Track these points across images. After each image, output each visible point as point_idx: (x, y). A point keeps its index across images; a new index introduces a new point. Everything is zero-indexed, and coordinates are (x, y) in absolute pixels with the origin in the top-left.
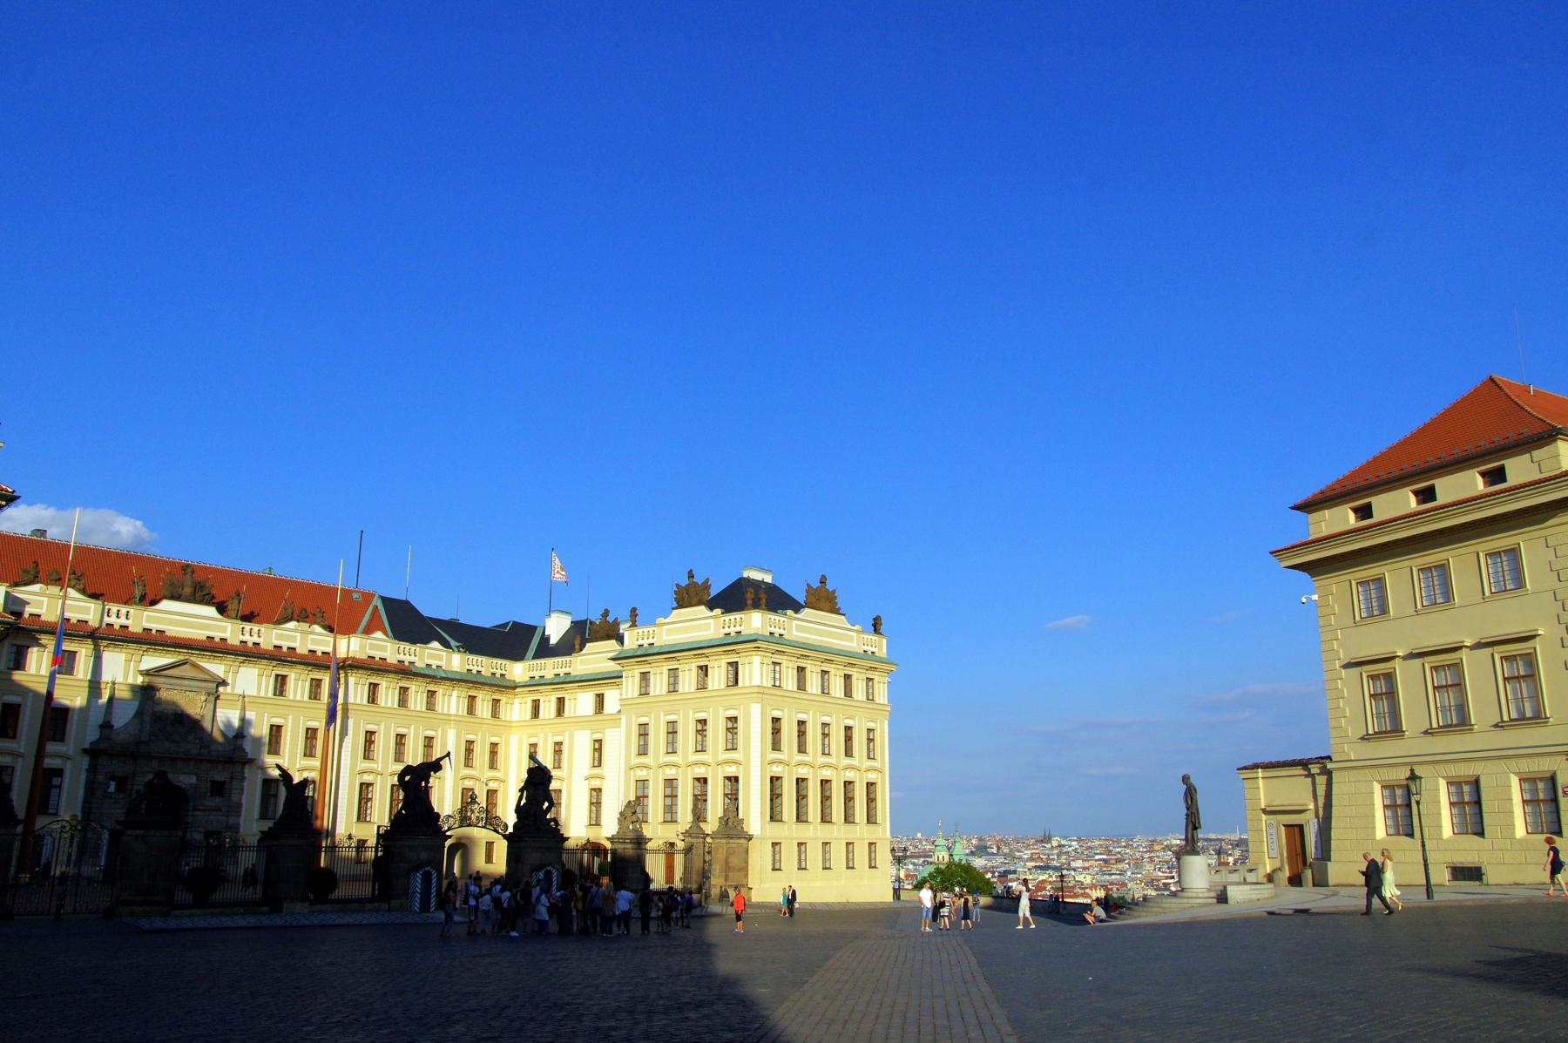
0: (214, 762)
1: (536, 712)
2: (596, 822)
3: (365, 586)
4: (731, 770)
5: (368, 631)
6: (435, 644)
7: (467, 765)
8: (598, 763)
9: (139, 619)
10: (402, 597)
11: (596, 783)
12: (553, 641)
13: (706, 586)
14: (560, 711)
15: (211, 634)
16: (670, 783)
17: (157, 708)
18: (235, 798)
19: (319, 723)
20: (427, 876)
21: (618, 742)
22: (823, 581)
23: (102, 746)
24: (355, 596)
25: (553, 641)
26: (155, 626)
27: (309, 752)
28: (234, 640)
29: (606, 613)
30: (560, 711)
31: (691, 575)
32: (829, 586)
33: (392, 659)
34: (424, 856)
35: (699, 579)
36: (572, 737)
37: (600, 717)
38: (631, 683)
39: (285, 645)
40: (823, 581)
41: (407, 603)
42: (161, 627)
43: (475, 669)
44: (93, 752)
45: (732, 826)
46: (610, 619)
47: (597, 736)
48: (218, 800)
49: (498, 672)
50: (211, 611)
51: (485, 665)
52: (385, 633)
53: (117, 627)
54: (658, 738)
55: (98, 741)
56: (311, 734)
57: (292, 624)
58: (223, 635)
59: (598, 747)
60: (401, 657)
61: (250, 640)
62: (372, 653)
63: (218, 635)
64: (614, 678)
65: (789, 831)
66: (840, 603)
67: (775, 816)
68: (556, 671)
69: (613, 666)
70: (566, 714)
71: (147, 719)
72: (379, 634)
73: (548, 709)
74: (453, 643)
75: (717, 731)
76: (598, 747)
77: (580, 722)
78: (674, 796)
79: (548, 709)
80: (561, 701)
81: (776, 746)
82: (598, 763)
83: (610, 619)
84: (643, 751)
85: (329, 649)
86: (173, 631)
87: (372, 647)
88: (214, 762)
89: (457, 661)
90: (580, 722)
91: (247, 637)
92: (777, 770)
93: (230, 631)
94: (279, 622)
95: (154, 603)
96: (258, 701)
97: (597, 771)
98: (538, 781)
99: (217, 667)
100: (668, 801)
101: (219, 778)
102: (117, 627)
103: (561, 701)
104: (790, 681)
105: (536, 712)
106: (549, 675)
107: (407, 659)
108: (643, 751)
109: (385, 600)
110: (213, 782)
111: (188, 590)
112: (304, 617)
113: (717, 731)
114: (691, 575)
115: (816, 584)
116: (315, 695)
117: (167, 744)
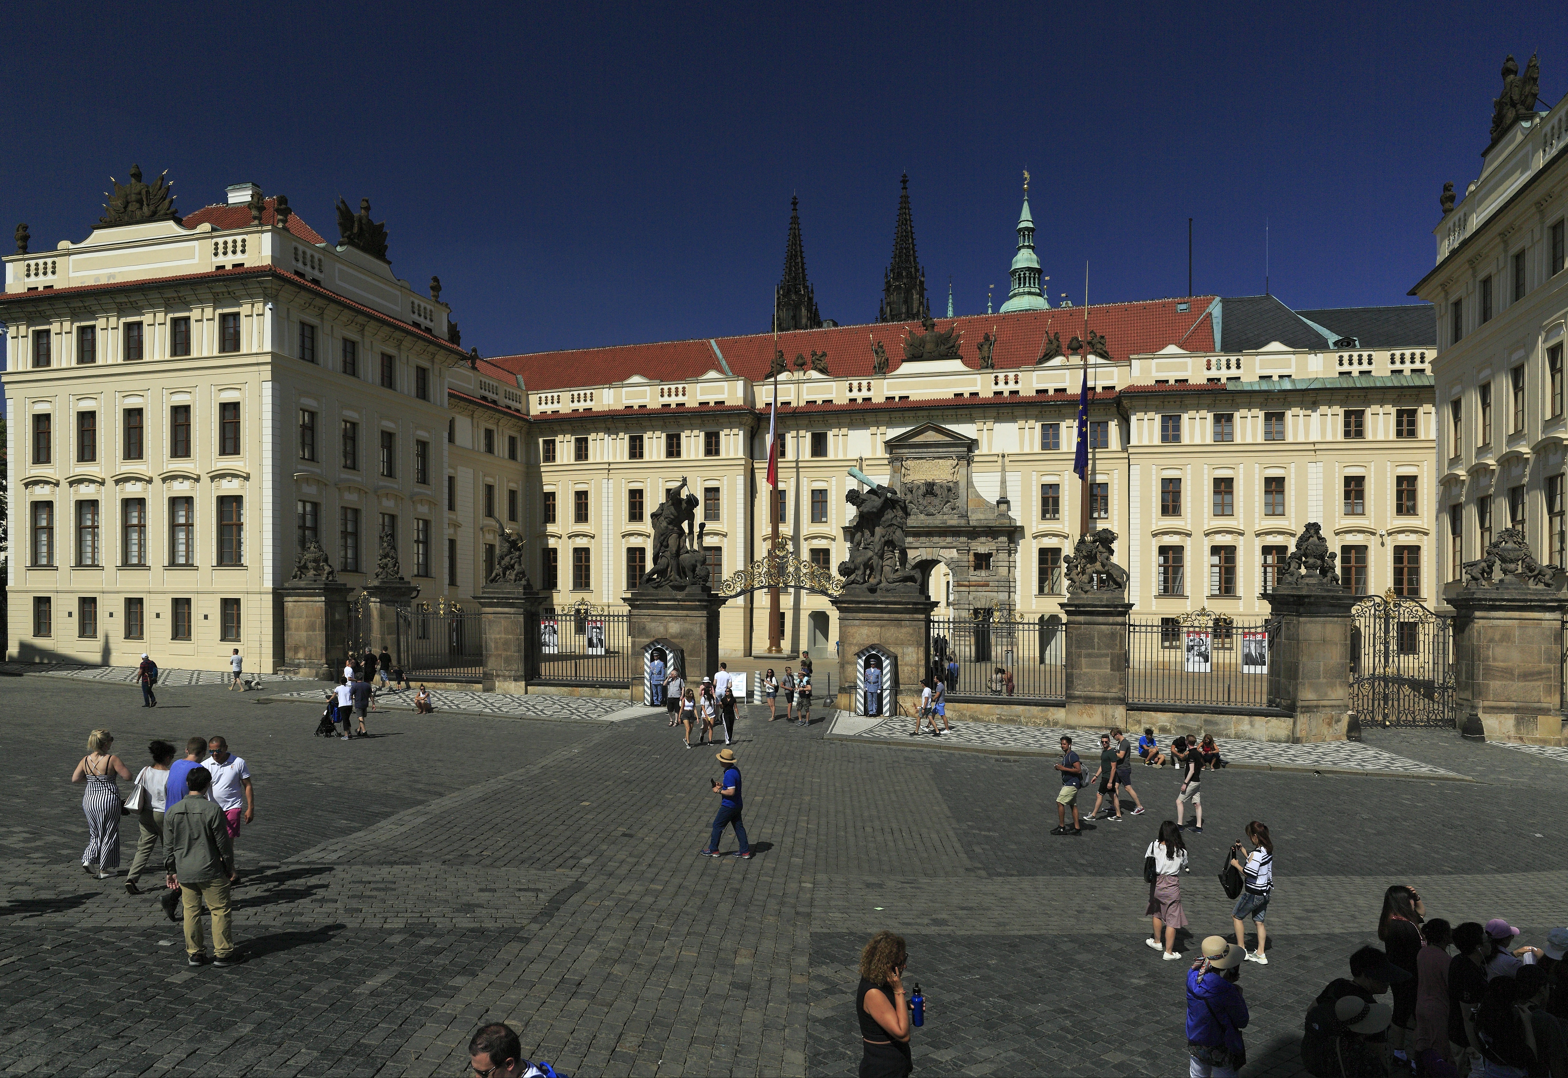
7: (1350, 512)
9: (881, 390)
15: (959, 390)
17: (908, 479)
18: (1003, 571)
26: (897, 394)
34: (674, 628)
39: (1051, 387)
42: (904, 393)
43: (1355, 369)
48: (983, 573)
51: (1381, 364)
53: (860, 401)
57: (1058, 361)
60: (1213, 373)
61: (1006, 389)
62: (1162, 376)
63: (966, 391)
74: (1332, 338)
89: (1318, 367)
91: (1001, 387)
94: (1041, 362)
96: (1022, 459)
101: (982, 550)
102: (860, 401)
107: (1223, 374)
110: (976, 555)
111: (929, 347)
112: (1075, 348)
117: (922, 517)
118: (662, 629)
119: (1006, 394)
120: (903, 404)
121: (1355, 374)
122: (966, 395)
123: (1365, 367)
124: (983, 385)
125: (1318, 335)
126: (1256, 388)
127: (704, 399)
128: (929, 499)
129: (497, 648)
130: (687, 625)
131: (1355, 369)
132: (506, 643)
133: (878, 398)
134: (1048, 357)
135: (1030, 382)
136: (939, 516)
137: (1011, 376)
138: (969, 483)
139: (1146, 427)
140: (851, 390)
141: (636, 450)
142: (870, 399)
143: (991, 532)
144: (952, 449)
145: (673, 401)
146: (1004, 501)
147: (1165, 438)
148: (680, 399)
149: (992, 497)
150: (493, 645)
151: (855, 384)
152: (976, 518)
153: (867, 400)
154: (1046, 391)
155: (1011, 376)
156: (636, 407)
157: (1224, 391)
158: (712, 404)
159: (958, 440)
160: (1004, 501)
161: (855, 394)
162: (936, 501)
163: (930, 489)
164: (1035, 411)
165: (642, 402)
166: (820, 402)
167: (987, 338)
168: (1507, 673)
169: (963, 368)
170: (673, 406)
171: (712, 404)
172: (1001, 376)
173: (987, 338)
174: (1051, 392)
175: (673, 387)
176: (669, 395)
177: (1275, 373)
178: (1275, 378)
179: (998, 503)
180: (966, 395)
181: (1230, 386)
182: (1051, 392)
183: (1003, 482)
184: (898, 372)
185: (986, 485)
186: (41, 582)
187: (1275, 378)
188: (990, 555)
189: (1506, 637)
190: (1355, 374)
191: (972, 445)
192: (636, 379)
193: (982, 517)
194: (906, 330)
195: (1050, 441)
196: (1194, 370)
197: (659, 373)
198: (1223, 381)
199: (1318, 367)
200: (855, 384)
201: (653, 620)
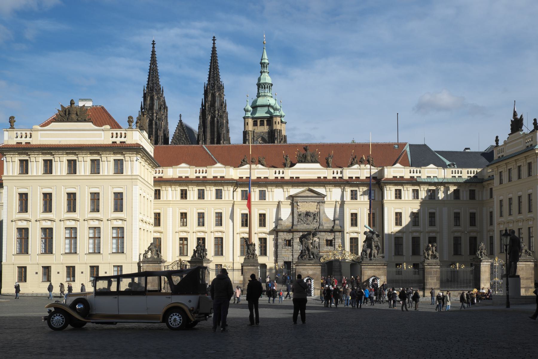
3: (401, 141)
7: (456, 225)
9: (289, 173)
13: (521, 119)
15: (319, 176)
24: (396, 146)
26: (294, 176)
28: (330, 177)
33: (407, 176)
35: (519, 117)
39: (354, 176)
41: (425, 145)
42: (297, 176)
43: (457, 175)
44: (275, 232)
48: (329, 247)
50: (318, 165)
53: (279, 178)
57: (356, 166)
58: (325, 176)
60: (412, 175)
74: (448, 163)
86: (303, 176)
87: (394, 172)
93: (329, 173)
95: (292, 165)
99: (321, 190)
101: (329, 238)
102: (279, 178)
107: (415, 175)
109: (410, 146)
110: (327, 240)
112: (361, 162)
114: (515, 114)
117: (305, 225)
121: (457, 177)
122: (322, 178)
123: (460, 175)
124: (329, 173)
125: (443, 161)
126: (426, 181)
127: (215, 175)
131: (457, 175)
134: (352, 164)
136: (312, 225)
138: (324, 212)
139: (389, 193)
140: (275, 173)
141: (184, 195)
142: (283, 178)
143: (332, 231)
144: (317, 198)
145: (201, 175)
147: (396, 198)
148: (204, 175)
152: (327, 226)
154: (352, 178)
156: (184, 177)
159: (319, 195)
161: (277, 175)
162: (311, 219)
163: (307, 214)
165: (187, 175)
170: (201, 177)
174: (354, 178)
178: (432, 177)
180: (322, 178)
181: (418, 180)
182: (354, 178)
186: (23, 260)
187: (432, 177)
188: (332, 240)
190: (457, 177)
191: (324, 196)
192: (183, 165)
193: (328, 225)
197: (192, 163)
198: (415, 177)
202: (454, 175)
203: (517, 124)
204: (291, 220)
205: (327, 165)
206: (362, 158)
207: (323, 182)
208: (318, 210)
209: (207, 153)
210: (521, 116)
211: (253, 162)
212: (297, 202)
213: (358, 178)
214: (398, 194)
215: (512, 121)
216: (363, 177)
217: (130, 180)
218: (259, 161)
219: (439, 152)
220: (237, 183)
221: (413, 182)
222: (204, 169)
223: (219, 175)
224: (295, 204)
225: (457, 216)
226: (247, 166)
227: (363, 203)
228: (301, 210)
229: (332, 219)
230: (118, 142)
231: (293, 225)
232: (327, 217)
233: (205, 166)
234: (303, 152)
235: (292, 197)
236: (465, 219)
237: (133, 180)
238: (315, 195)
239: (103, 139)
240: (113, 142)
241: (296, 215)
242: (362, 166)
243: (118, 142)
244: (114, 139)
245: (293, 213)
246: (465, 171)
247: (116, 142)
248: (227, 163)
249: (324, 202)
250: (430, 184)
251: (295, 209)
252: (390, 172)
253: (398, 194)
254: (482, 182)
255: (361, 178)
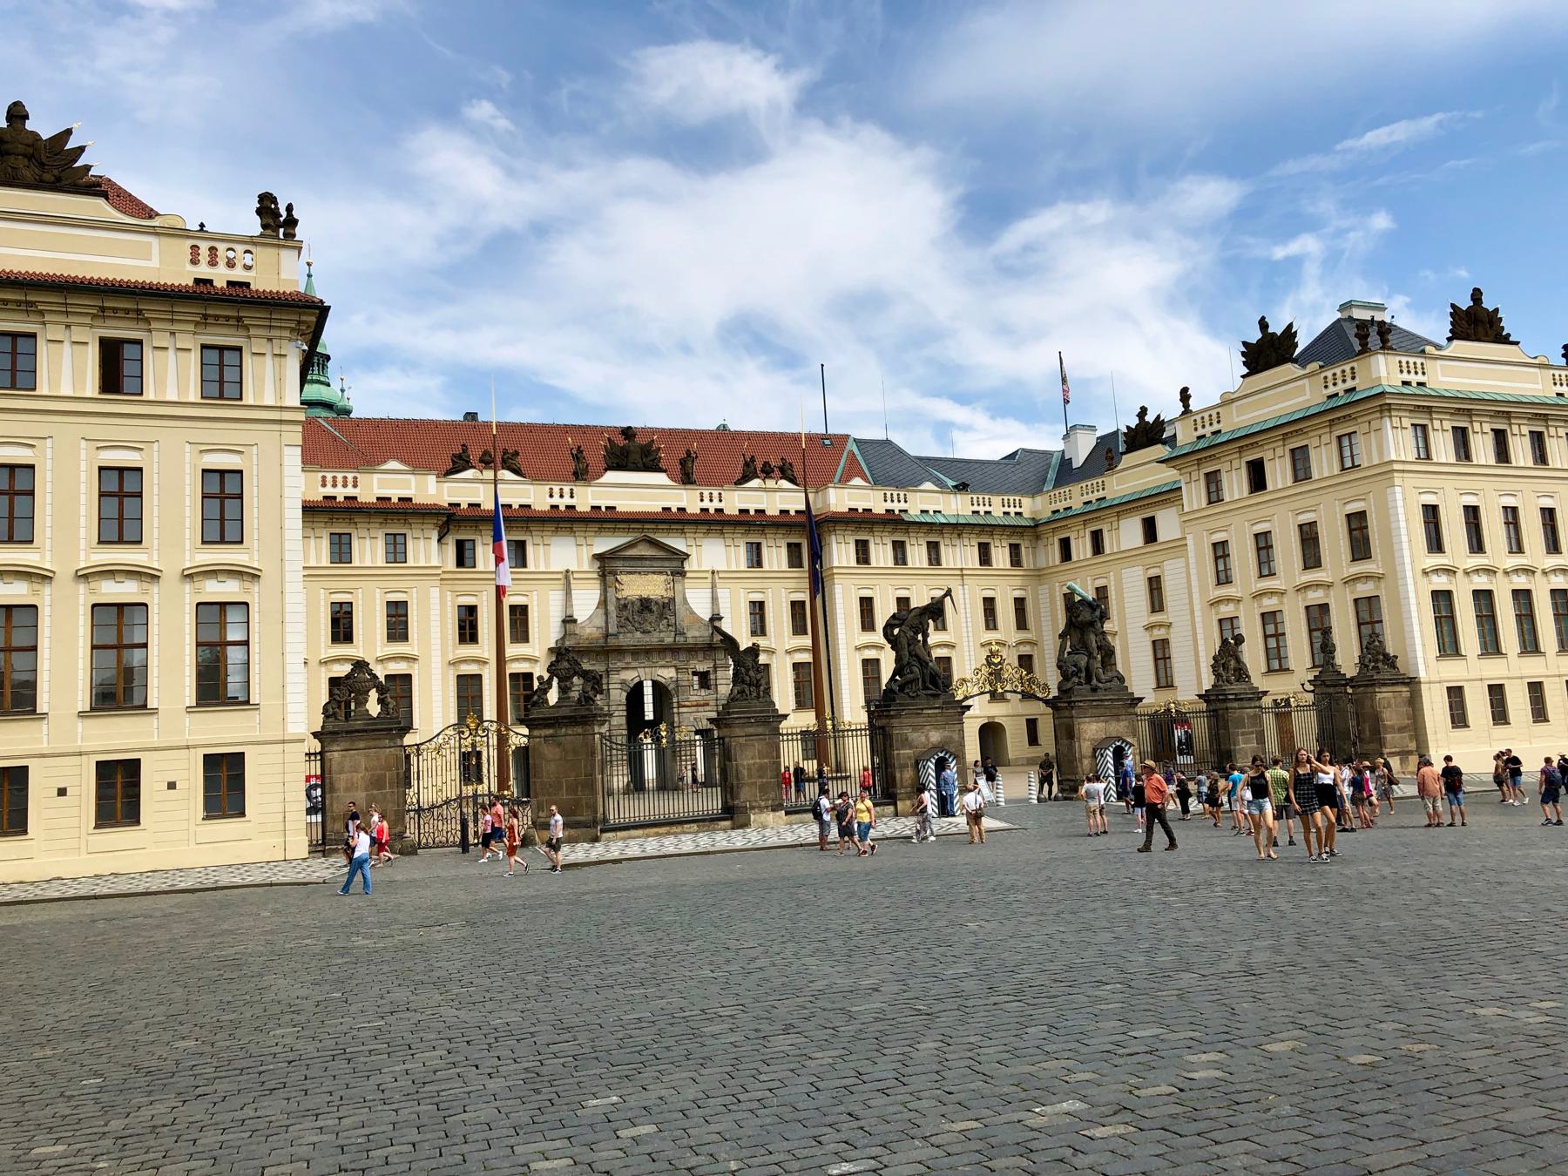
0: (693, 650)
1: (1066, 555)
2: (1164, 681)
4: (1364, 589)
5: (845, 480)
6: (928, 486)
8: (1157, 604)
9: (586, 498)
10: (882, 437)
11: (1159, 634)
12: (1078, 462)
13: (1289, 333)
14: (1098, 548)
16: (1269, 618)
19: (804, 596)
20: (941, 765)
21: (1188, 578)
22: (1477, 295)
23: (567, 643)
25: (1078, 462)
26: (603, 503)
27: (799, 629)
28: (694, 508)
29: (1143, 411)
30: (1098, 548)
31: (1263, 324)
32: (1488, 304)
33: (879, 508)
34: (935, 737)
35: (1277, 328)
36: (1119, 580)
37: (1152, 547)
38: (1194, 495)
40: (1477, 295)
41: (888, 442)
43: (982, 509)
45: (1380, 662)
46: (1150, 418)
47: (1153, 573)
48: (703, 692)
49: (1012, 510)
52: (866, 480)
54: (1243, 557)
55: (563, 639)
56: (797, 607)
57: (756, 483)
58: (681, 505)
59: (1155, 585)
60: (889, 505)
61: (711, 507)
64: (1170, 495)
65: (1473, 671)
66: (1508, 326)
67: (1449, 646)
68: (1086, 498)
69: (1167, 475)
70: (1107, 550)
71: (611, 608)
72: (857, 481)
73: (1081, 548)
74: (951, 483)
75: (1334, 542)
76: (1155, 585)
77: (1127, 556)
78: (1279, 635)
79: (1081, 548)
80: (1097, 538)
81: (1436, 543)
82: (1157, 604)
83: (1150, 418)
84: (1223, 578)
85: (803, 507)
88: (693, 650)
89: (957, 507)
90: (1127, 556)
91: (706, 504)
92: (1441, 582)
96: (733, 576)
97: (1158, 617)
98: (1085, 620)
100: (1272, 643)
101: (701, 668)
102: (562, 508)
103: (1097, 538)
104: (1443, 446)
105: (1066, 555)
106: (1077, 504)
107: (896, 507)
108: (1223, 578)
112: (767, 472)
113: (1334, 542)
114: (1263, 324)
115: (1465, 303)
116: (794, 560)
118: (923, 739)
119: (712, 511)
120: (609, 515)
122: (674, 510)
123: (987, 508)
124: (690, 500)
128: (648, 616)
129: (750, 776)
130: (946, 733)
131: (982, 509)
132: (761, 768)
133: (583, 507)
134: (745, 478)
135: (734, 501)
136: (656, 634)
137: (715, 494)
139: (841, 552)
144: (667, 564)
145: (340, 493)
146: (716, 618)
148: (350, 491)
149: (706, 615)
150: (745, 772)
151: (556, 489)
152: (695, 634)
153: (570, 508)
155: (715, 494)
157: (902, 522)
158: (395, 500)
160: (716, 618)
161: (556, 500)
162: (651, 618)
163: (645, 604)
164: (741, 530)
166: (516, 506)
167: (688, 453)
168: (1392, 729)
169: (668, 482)
170: (340, 499)
171: (395, 500)
172: (706, 493)
173: (688, 453)
175: (340, 476)
176: (335, 485)
177: (931, 509)
179: (712, 620)
180: (674, 510)
181: (905, 517)
183: (714, 599)
184: (604, 479)
185: (697, 601)
189: (1389, 705)
193: (697, 634)
194: (640, 440)
195: (756, 560)
196: (875, 501)
199: (957, 507)
200: (556, 489)
201: (914, 730)
202: (976, 508)
203: (1267, 352)
204: (600, 622)
205: (686, 478)
206: (766, 464)
207: (677, 521)
208: (670, 594)
209: (335, 438)
210: (1290, 326)
211: (487, 462)
212: (614, 574)
213: (760, 512)
214: (863, 556)
215: (1245, 344)
216: (773, 511)
217: (276, 427)
218: (504, 461)
219: (921, 459)
220: (448, 520)
221: (893, 522)
222: (350, 476)
223: (395, 493)
224: (610, 578)
225: (989, 604)
226: (469, 474)
227: (776, 577)
228: (625, 594)
229: (706, 616)
230: (220, 283)
231: (607, 635)
232: (693, 613)
233: (354, 468)
234: (621, 441)
235: (599, 557)
236: (1005, 613)
237: (284, 427)
238: (661, 554)
239: (155, 263)
240: (198, 281)
241: (611, 608)
242: (770, 483)
243: (220, 283)
244: (204, 271)
245: (603, 603)
246: (996, 500)
247: (210, 282)
248: (418, 464)
249: (683, 574)
250: (930, 527)
251: (611, 591)
252: (839, 499)
253: (863, 556)
254: (1037, 526)
255: (768, 513)
